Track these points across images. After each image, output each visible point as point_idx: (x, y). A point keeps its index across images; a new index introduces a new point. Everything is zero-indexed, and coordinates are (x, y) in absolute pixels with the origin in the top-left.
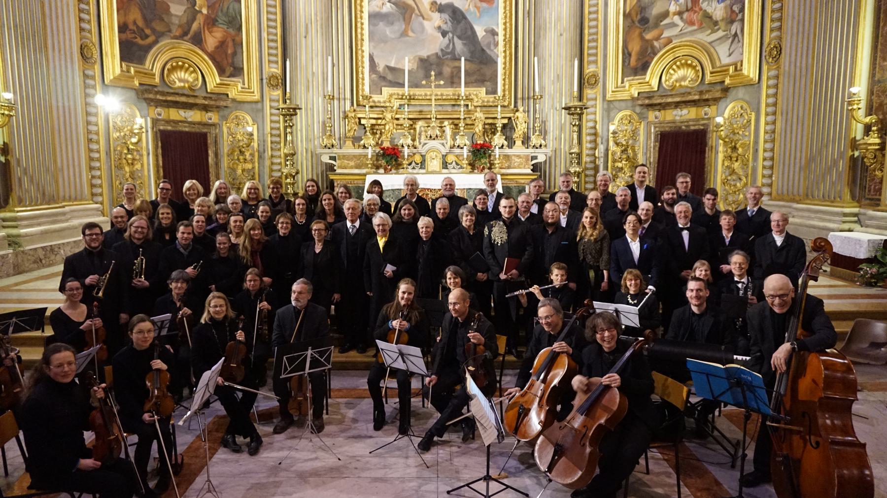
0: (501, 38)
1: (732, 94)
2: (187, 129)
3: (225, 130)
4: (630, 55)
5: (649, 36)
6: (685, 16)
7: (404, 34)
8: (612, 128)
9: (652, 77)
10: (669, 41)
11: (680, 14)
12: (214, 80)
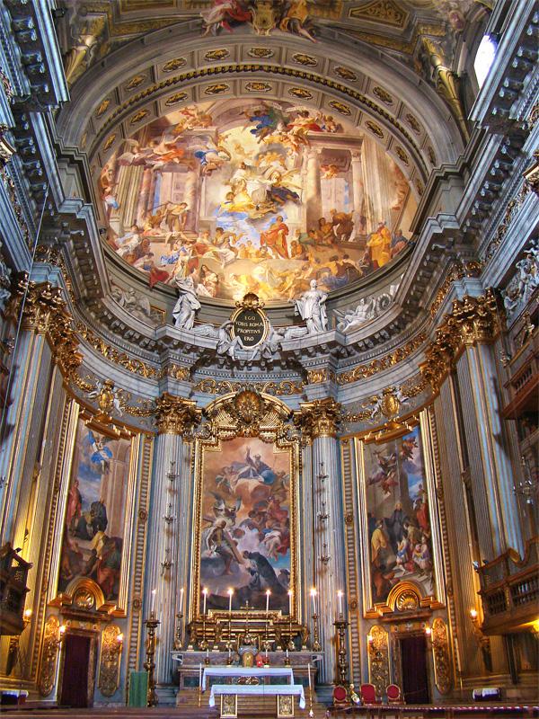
0: (292, 577)
1: (434, 614)
2: (81, 635)
3: (103, 636)
4: (376, 588)
5: (386, 577)
6: (406, 565)
7: (225, 573)
8: (370, 638)
9: (391, 604)
10: (398, 580)
11: (403, 564)
12: (101, 602)
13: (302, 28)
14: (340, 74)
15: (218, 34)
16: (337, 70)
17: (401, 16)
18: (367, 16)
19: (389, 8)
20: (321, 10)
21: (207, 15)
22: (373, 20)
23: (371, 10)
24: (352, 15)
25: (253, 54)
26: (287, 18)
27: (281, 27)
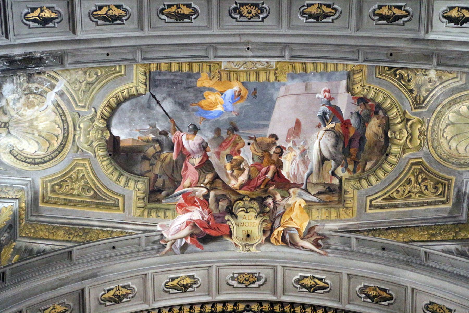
13: (302, 239)
14: (368, 296)
15: (182, 253)
16: (362, 291)
17: (444, 185)
18: (393, 202)
19: (423, 180)
20: (326, 209)
21: (168, 227)
22: (403, 206)
23: (398, 192)
24: (371, 207)
25: (235, 283)
26: (281, 229)
27: (272, 240)
